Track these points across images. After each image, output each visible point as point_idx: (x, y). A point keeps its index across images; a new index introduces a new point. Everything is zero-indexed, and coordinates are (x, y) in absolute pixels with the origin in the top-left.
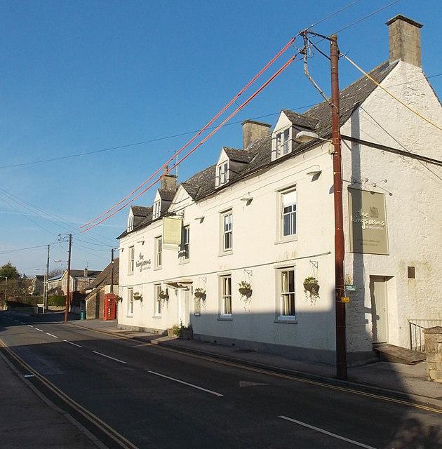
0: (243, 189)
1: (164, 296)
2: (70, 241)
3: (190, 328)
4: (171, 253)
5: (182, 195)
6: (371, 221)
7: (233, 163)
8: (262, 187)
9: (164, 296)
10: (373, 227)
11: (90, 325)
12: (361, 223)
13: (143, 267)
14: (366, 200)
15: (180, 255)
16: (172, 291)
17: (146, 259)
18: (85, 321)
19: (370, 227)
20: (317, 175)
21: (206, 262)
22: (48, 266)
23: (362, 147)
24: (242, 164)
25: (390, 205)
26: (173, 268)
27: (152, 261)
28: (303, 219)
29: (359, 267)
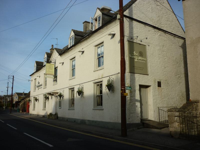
0: (80, 47)
1: (47, 98)
2: (13, 78)
3: (56, 114)
4: (50, 80)
5: (55, 55)
6: (140, 58)
7: (76, 36)
8: (88, 46)
9: (47, 98)
10: (141, 61)
11: (22, 116)
12: (134, 59)
13: (39, 87)
14: (135, 46)
15: (54, 81)
16: (50, 97)
17: (40, 84)
18: (19, 113)
19: (139, 61)
20: (114, 35)
21: (64, 85)
22: (7, 91)
23: (135, 23)
24: (80, 37)
25: (149, 51)
26: (51, 87)
27: (43, 85)
28: (106, 60)
29: (133, 80)
